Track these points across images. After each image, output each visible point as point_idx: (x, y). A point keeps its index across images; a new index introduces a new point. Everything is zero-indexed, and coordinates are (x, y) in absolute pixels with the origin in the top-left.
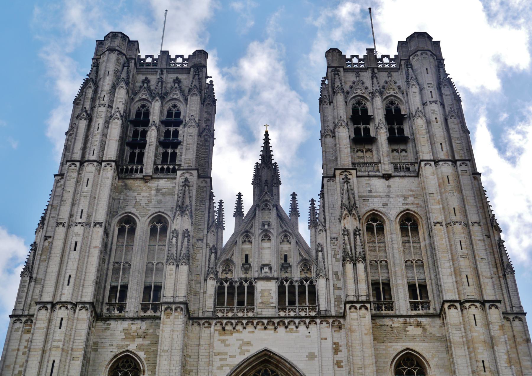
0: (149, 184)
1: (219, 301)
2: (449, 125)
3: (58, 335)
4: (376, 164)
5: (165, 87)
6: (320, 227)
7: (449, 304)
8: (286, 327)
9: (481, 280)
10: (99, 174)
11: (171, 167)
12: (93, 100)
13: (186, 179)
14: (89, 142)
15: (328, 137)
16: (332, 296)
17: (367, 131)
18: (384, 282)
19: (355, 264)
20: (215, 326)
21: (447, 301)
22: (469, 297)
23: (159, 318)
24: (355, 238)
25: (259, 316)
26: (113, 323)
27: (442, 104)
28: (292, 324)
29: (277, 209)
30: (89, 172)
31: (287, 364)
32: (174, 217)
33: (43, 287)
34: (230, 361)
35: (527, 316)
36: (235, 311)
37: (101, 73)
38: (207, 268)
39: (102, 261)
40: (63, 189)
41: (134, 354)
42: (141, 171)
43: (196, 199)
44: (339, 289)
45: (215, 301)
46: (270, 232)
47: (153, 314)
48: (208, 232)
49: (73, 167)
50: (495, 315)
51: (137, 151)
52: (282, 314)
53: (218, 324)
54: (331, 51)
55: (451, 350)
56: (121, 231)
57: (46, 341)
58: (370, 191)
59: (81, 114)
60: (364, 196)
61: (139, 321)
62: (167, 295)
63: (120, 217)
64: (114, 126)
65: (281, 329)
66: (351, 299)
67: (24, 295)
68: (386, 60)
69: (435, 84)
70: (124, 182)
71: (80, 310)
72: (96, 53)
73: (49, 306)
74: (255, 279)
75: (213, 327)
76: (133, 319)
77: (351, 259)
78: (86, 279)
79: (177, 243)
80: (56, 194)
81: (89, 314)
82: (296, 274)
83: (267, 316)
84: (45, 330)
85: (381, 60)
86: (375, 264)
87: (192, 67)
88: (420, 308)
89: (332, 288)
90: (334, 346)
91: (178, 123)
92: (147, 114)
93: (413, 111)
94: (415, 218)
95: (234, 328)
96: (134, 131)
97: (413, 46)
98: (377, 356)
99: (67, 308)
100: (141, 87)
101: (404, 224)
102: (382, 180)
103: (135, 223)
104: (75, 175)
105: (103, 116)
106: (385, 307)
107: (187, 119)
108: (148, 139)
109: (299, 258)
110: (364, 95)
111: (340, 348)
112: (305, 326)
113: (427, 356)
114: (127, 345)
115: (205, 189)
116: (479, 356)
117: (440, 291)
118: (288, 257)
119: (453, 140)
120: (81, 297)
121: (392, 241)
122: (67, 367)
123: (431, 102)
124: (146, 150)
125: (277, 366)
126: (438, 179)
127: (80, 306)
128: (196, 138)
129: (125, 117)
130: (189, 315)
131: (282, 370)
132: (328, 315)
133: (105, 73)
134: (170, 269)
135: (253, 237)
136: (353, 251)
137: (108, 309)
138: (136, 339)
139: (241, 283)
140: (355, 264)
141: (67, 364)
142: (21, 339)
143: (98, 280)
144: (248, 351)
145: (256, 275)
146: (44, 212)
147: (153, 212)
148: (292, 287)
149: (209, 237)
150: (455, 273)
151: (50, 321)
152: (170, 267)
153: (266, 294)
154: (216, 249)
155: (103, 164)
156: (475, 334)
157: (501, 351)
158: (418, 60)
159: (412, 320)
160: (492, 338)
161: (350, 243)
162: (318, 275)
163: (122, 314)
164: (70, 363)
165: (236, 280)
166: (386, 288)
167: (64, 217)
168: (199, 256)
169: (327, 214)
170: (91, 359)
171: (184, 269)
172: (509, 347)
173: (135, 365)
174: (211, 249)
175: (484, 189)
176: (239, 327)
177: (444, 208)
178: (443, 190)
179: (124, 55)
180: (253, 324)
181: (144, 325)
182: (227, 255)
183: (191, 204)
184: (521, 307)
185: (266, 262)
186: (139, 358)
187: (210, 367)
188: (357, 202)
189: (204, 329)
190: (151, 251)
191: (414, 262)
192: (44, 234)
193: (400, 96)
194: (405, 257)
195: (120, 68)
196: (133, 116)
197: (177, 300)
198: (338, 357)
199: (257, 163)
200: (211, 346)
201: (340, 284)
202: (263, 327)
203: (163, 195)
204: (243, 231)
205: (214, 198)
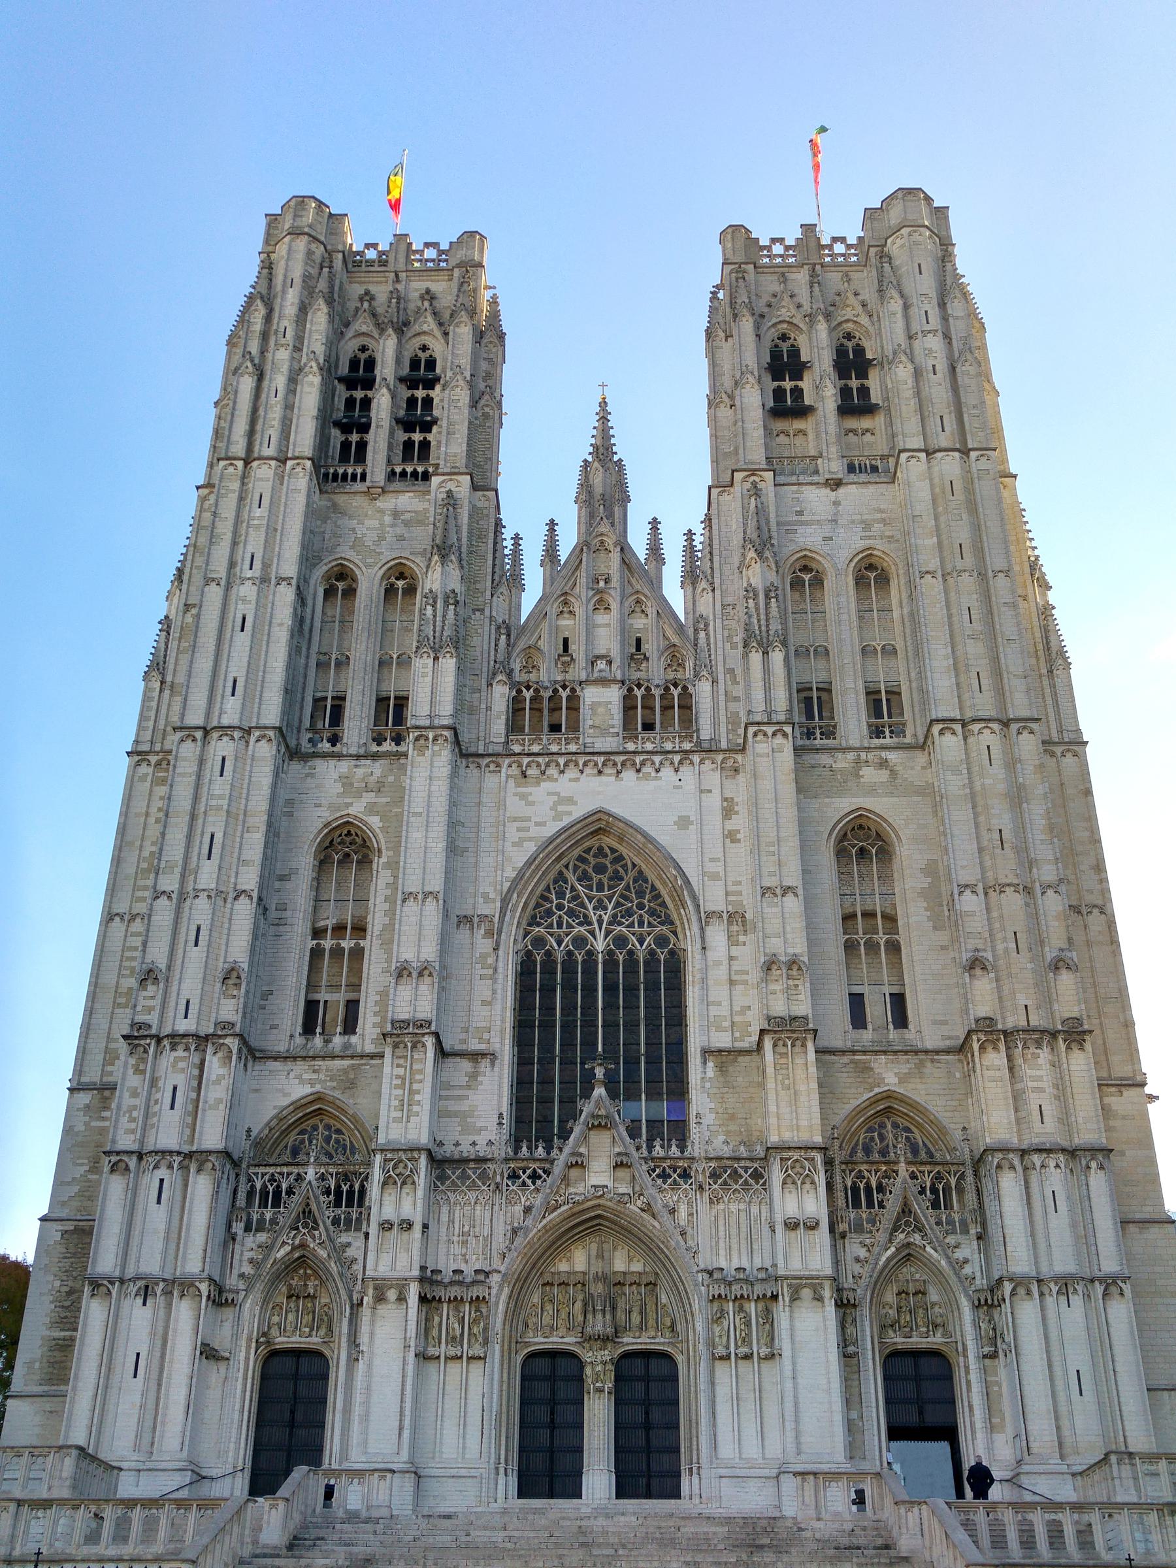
0: (378, 503)
1: (514, 726)
2: (959, 379)
3: (220, 787)
4: (814, 458)
5: (405, 309)
6: (703, 584)
7: (941, 726)
8: (638, 771)
9: (1005, 680)
10: (282, 484)
11: (420, 469)
12: (265, 336)
13: (450, 494)
14: (261, 421)
16: (722, 712)
17: (798, 392)
18: (821, 686)
19: (766, 653)
20: (508, 769)
22: (980, 713)
23: (405, 755)
24: (767, 605)
25: (588, 750)
26: (320, 764)
27: (947, 336)
29: (622, 549)
30: (261, 480)
32: (428, 567)
33: (186, 700)
34: (534, 832)
35: (1088, 749)
36: (545, 741)
37: (279, 280)
38: (492, 663)
39: (295, 651)
40: (215, 514)
41: (361, 821)
42: (364, 477)
43: (470, 532)
44: (737, 699)
45: (507, 724)
47: (395, 748)
48: (492, 595)
49: (231, 469)
50: (1028, 744)
51: (354, 437)
52: (631, 746)
55: (942, 810)
56: (329, 593)
57: (196, 799)
58: (800, 513)
59: (242, 364)
60: (788, 523)
61: (368, 762)
62: (418, 711)
63: (325, 568)
64: (307, 389)
65: (629, 775)
66: (758, 718)
67: (152, 714)
68: (839, 248)
69: (933, 294)
70: (330, 500)
71: (258, 741)
72: (267, 242)
73: (199, 734)
74: (581, 683)
75: (503, 770)
76: (358, 757)
77: (760, 644)
78: (266, 685)
79: (435, 616)
80: (203, 524)
81: (275, 748)
82: (655, 671)
84: (194, 777)
85: (830, 247)
86: (802, 652)
87: (458, 266)
88: (887, 733)
89: (722, 698)
90: (725, 804)
91: (430, 384)
92: (371, 364)
93: (889, 352)
94: (885, 564)
96: (347, 399)
97: (895, 215)
98: (803, 823)
99: (233, 738)
100: (357, 309)
101: (863, 577)
102: (826, 491)
103: (355, 580)
104: (236, 485)
105: (285, 368)
106: (822, 734)
107: (449, 374)
108: (373, 414)
109: (663, 644)
110: (795, 321)
111: (736, 808)
113: (896, 820)
114: (348, 805)
115: (485, 512)
116: (993, 822)
117: (925, 702)
119: (964, 409)
120: (258, 718)
121: (839, 609)
122: (237, 845)
123: (925, 333)
124: (370, 437)
125: (621, 839)
126: (932, 486)
127: (257, 733)
128: (466, 411)
129: (328, 368)
130: (460, 750)
132: (714, 748)
133: (284, 281)
134: (422, 664)
135: (576, 605)
136: (763, 628)
137: (310, 740)
138: (364, 794)
139: (555, 691)
140: (766, 653)
141: (238, 839)
142: (150, 795)
143: (289, 687)
145: (583, 677)
146: (182, 558)
147: (390, 558)
149: (494, 604)
150: (956, 669)
151: (201, 762)
152: (422, 661)
153: (601, 710)
154: (508, 628)
155: (290, 463)
156: (988, 781)
157: (1037, 813)
158: (902, 246)
159: (871, 756)
160: (1020, 788)
161: (758, 615)
162: (697, 675)
163: (337, 749)
164: (242, 837)
165: (547, 684)
166: (824, 696)
167: (219, 567)
168: (475, 641)
169: (716, 559)
170: (282, 830)
171: (449, 664)
172: (1050, 805)
173: (364, 840)
174: (499, 628)
175: (1022, 507)
176: (552, 771)
177: (940, 543)
178: (941, 509)
179: (322, 243)
180: (577, 765)
181: (377, 769)
182: (529, 639)
183: (459, 540)
184: (1078, 731)
185: (601, 651)
187: (501, 842)
188: (774, 534)
189: (488, 774)
190: (386, 631)
191: (879, 649)
192: (183, 601)
193: (864, 320)
194: (861, 639)
195: (314, 271)
196: (344, 369)
197: (436, 722)
198: (731, 825)
199: (585, 461)
200: (501, 804)
201: (738, 691)
202: (596, 771)
203: (407, 524)
204: (559, 593)
205: (503, 530)
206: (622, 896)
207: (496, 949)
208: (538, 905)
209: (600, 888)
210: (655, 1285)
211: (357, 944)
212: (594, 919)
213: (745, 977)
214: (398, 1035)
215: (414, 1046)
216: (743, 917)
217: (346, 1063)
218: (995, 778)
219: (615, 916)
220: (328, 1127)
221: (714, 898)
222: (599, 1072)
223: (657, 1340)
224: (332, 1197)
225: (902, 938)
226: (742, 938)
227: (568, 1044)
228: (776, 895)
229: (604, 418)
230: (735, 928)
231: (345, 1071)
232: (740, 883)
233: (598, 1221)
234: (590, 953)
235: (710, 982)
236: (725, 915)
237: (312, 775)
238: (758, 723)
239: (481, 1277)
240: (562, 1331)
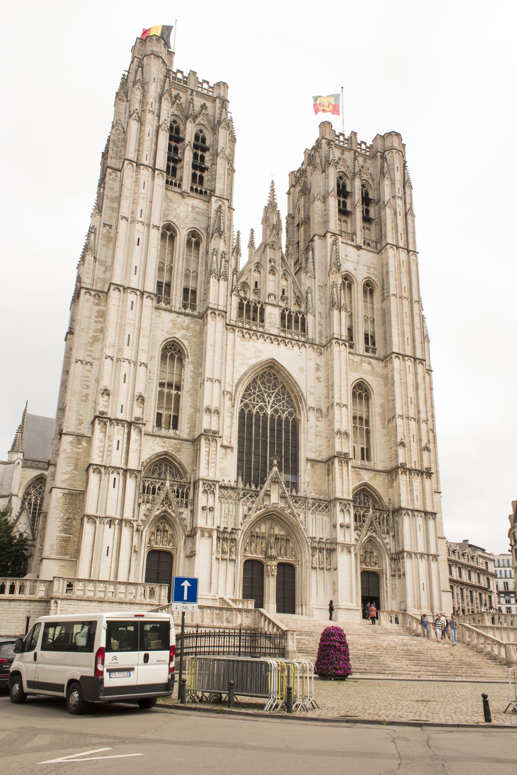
1: (240, 315)
6: (309, 274)
8: (286, 345)
15: (319, 201)
16: (317, 329)
19: (340, 311)
21: (395, 353)
25: (268, 332)
26: (163, 314)
28: (290, 343)
31: (286, 372)
41: (180, 341)
46: (276, 268)
47: (192, 313)
52: (283, 334)
53: (240, 332)
54: (326, 123)
58: (346, 256)
65: (282, 345)
74: (265, 303)
75: (236, 333)
83: (273, 333)
89: (317, 323)
95: (251, 338)
112: (298, 347)
118: (285, 291)
125: (278, 372)
131: (281, 374)
135: (262, 269)
139: (255, 304)
140: (340, 311)
144: (261, 357)
148: (290, 316)
153: (272, 316)
159: (366, 359)
163: (168, 307)
180: (264, 337)
186: (184, 345)
198: (319, 374)
199: (265, 207)
202: (270, 341)
204: (256, 262)
206: (277, 393)
207: (233, 406)
208: (246, 391)
209: (269, 389)
210: (289, 540)
211: (177, 393)
212: (267, 401)
213: (321, 434)
214: (206, 435)
215: (212, 441)
216: (321, 411)
217: (177, 441)
218: (410, 378)
219: (274, 401)
220: (166, 465)
221: (311, 401)
222: (275, 462)
223: (290, 559)
224: (176, 494)
225: (370, 428)
226: (320, 419)
227: (257, 448)
228: (340, 406)
229: (273, 190)
230: (318, 415)
231: (176, 445)
232: (320, 398)
233: (272, 516)
234: (265, 414)
235: (309, 434)
236: (315, 409)
237: (160, 317)
238: (337, 339)
239: (234, 531)
240: (258, 553)
